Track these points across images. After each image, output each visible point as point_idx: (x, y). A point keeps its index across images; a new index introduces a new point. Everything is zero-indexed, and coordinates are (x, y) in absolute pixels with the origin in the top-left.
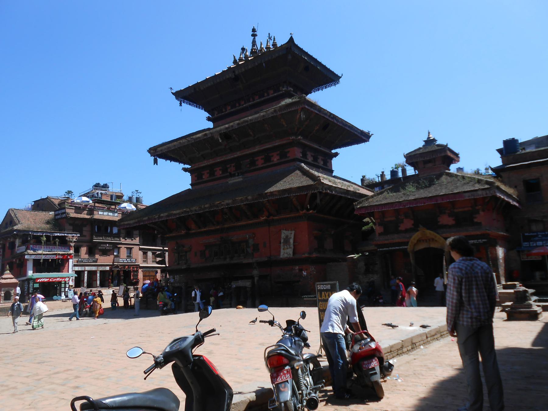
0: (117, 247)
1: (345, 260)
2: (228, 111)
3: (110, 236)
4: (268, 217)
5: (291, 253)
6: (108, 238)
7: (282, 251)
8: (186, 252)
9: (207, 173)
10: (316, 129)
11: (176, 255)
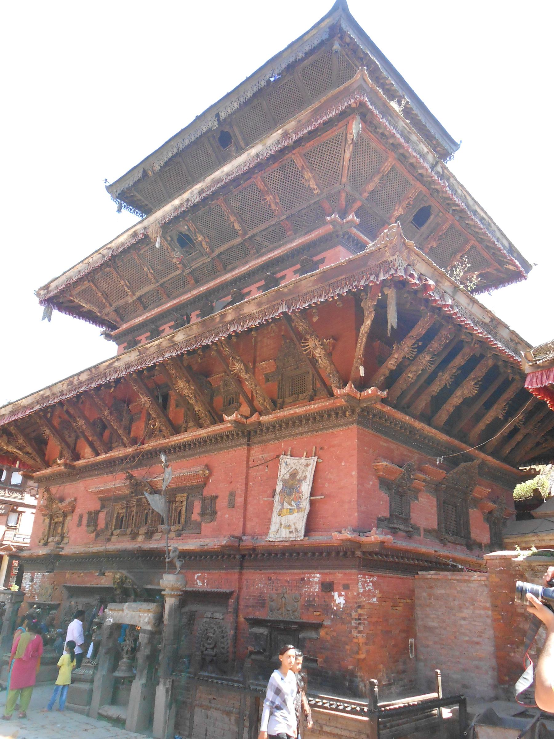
4: (247, 418)
5: (301, 526)
7: (275, 518)
8: (65, 515)
11: (47, 521)
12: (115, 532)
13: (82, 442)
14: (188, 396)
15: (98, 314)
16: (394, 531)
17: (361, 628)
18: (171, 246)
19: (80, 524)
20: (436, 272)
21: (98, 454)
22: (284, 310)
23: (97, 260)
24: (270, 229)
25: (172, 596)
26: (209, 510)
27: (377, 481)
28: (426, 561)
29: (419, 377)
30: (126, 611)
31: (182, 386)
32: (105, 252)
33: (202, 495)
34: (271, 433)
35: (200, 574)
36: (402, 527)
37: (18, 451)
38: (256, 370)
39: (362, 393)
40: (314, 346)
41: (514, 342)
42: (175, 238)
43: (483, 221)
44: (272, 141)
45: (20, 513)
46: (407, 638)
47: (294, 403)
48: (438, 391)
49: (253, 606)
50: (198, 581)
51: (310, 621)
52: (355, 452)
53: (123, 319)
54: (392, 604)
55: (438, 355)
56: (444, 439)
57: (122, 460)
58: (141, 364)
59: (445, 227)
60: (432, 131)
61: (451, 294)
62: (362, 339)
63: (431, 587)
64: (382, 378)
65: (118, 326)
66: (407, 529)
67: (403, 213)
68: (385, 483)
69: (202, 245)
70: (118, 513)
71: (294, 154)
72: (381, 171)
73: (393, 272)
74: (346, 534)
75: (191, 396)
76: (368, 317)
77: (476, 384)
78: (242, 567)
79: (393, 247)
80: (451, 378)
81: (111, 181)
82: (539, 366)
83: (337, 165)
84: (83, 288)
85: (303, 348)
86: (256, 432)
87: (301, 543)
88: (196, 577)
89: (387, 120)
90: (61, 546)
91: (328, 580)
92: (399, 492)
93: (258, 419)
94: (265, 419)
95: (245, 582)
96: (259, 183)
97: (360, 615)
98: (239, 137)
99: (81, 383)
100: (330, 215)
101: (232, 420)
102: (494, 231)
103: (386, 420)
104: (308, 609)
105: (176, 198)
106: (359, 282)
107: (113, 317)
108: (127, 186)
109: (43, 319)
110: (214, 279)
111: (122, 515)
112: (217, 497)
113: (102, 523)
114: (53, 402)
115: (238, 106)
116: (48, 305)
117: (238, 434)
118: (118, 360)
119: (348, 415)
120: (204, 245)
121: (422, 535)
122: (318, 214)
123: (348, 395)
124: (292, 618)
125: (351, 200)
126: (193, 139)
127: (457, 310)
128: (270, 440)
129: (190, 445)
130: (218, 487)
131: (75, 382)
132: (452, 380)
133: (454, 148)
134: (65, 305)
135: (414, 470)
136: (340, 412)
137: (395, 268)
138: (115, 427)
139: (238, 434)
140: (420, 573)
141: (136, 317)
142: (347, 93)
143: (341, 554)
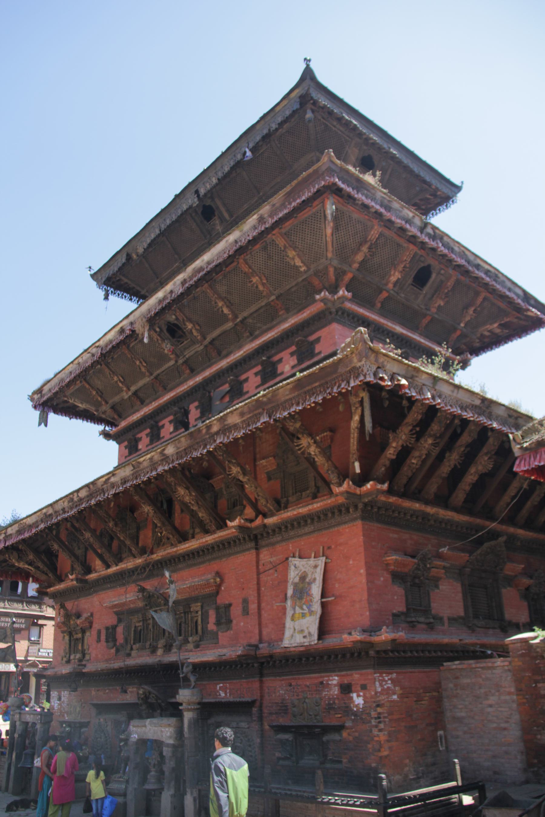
0: (36, 624)
1: (503, 651)
3: (22, 602)
4: (251, 521)
5: (314, 629)
6: (15, 605)
7: (289, 623)
8: (83, 631)
10: (393, 279)
11: (67, 638)
13: (91, 555)
14: (190, 503)
15: (95, 413)
16: (412, 626)
17: (382, 726)
18: (161, 337)
19: (99, 640)
20: (410, 368)
21: (108, 566)
22: (265, 420)
23: (87, 359)
24: (262, 311)
25: (189, 710)
26: (225, 619)
27: (389, 576)
28: (452, 652)
29: (424, 462)
30: (149, 727)
31: (183, 493)
32: (94, 350)
33: (216, 603)
34: (277, 535)
35: (221, 685)
36: (422, 619)
37: (30, 567)
38: (258, 469)
39: (362, 489)
40: (307, 444)
41: (513, 418)
42: (165, 329)
43: (489, 273)
44: (249, 227)
45: (42, 626)
46: (436, 730)
47: (298, 502)
48: (449, 472)
49: (276, 713)
50: (221, 692)
51: (332, 724)
52: (362, 549)
53: (121, 416)
54: (415, 699)
55: (441, 436)
56: (464, 519)
57: (132, 572)
58: (136, 478)
59: (450, 284)
60: (428, 179)
61: (431, 385)
62: (354, 434)
63: (457, 678)
64: (383, 469)
65: (116, 423)
66: (427, 621)
67: (400, 277)
68: (398, 577)
69: (192, 333)
70: (135, 627)
71: (274, 235)
72: (368, 239)
73: (362, 378)
74: (356, 636)
75: (193, 502)
76: (355, 413)
77: (489, 458)
78: (262, 675)
79: (359, 353)
80: (461, 457)
81: (96, 268)
82: (526, 449)
83: (320, 241)
84: (77, 387)
85: (297, 448)
86: (262, 535)
87: (315, 647)
88: (218, 688)
89: (363, 194)
90: (84, 663)
91: (346, 682)
92: (415, 584)
93: (263, 521)
94: (270, 521)
95: (267, 690)
96: (243, 265)
97: (379, 713)
98: (223, 210)
99: (81, 500)
100: (319, 292)
101: (236, 526)
102: (504, 282)
103: (393, 511)
104: (329, 712)
105: (159, 291)
106: (332, 388)
107: (110, 414)
108: (111, 272)
109: (40, 424)
110: (209, 366)
111: (139, 628)
112: (230, 605)
113: (120, 638)
114: (56, 520)
115: (217, 181)
116: (44, 409)
117: (244, 538)
118: (113, 475)
119: (351, 512)
120: (195, 333)
121: (446, 624)
122: (308, 292)
123: (347, 492)
124: (315, 723)
125: (340, 274)
126: (174, 218)
127: (439, 401)
128: (278, 542)
129: (198, 552)
130: (230, 594)
131: (76, 499)
132: (462, 459)
133: (456, 190)
134: (61, 406)
135: (429, 559)
136: (343, 509)
137: (364, 374)
138: (122, 538)
139: (244, 538)
140: (445, 664)
141: (134, 413)
142: (317, 175)
143: (356, 654)
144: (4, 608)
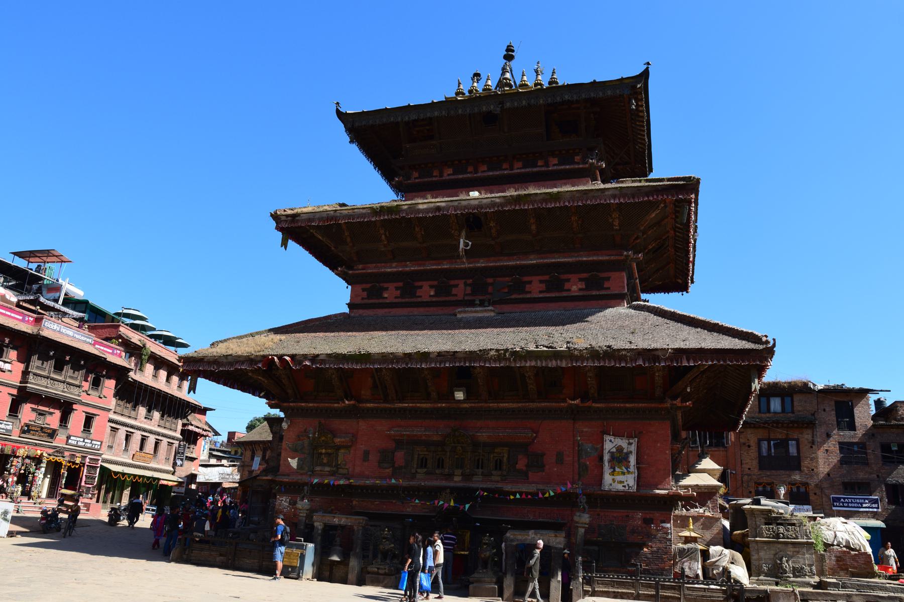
2: (446, 177)
7: (607, 478)
8: (338, 448)
9: (397, 288)
10: (650, 247)
12: (419, 470)
120: (493, 231)
138: (429, 384)
144: (47, 387)
